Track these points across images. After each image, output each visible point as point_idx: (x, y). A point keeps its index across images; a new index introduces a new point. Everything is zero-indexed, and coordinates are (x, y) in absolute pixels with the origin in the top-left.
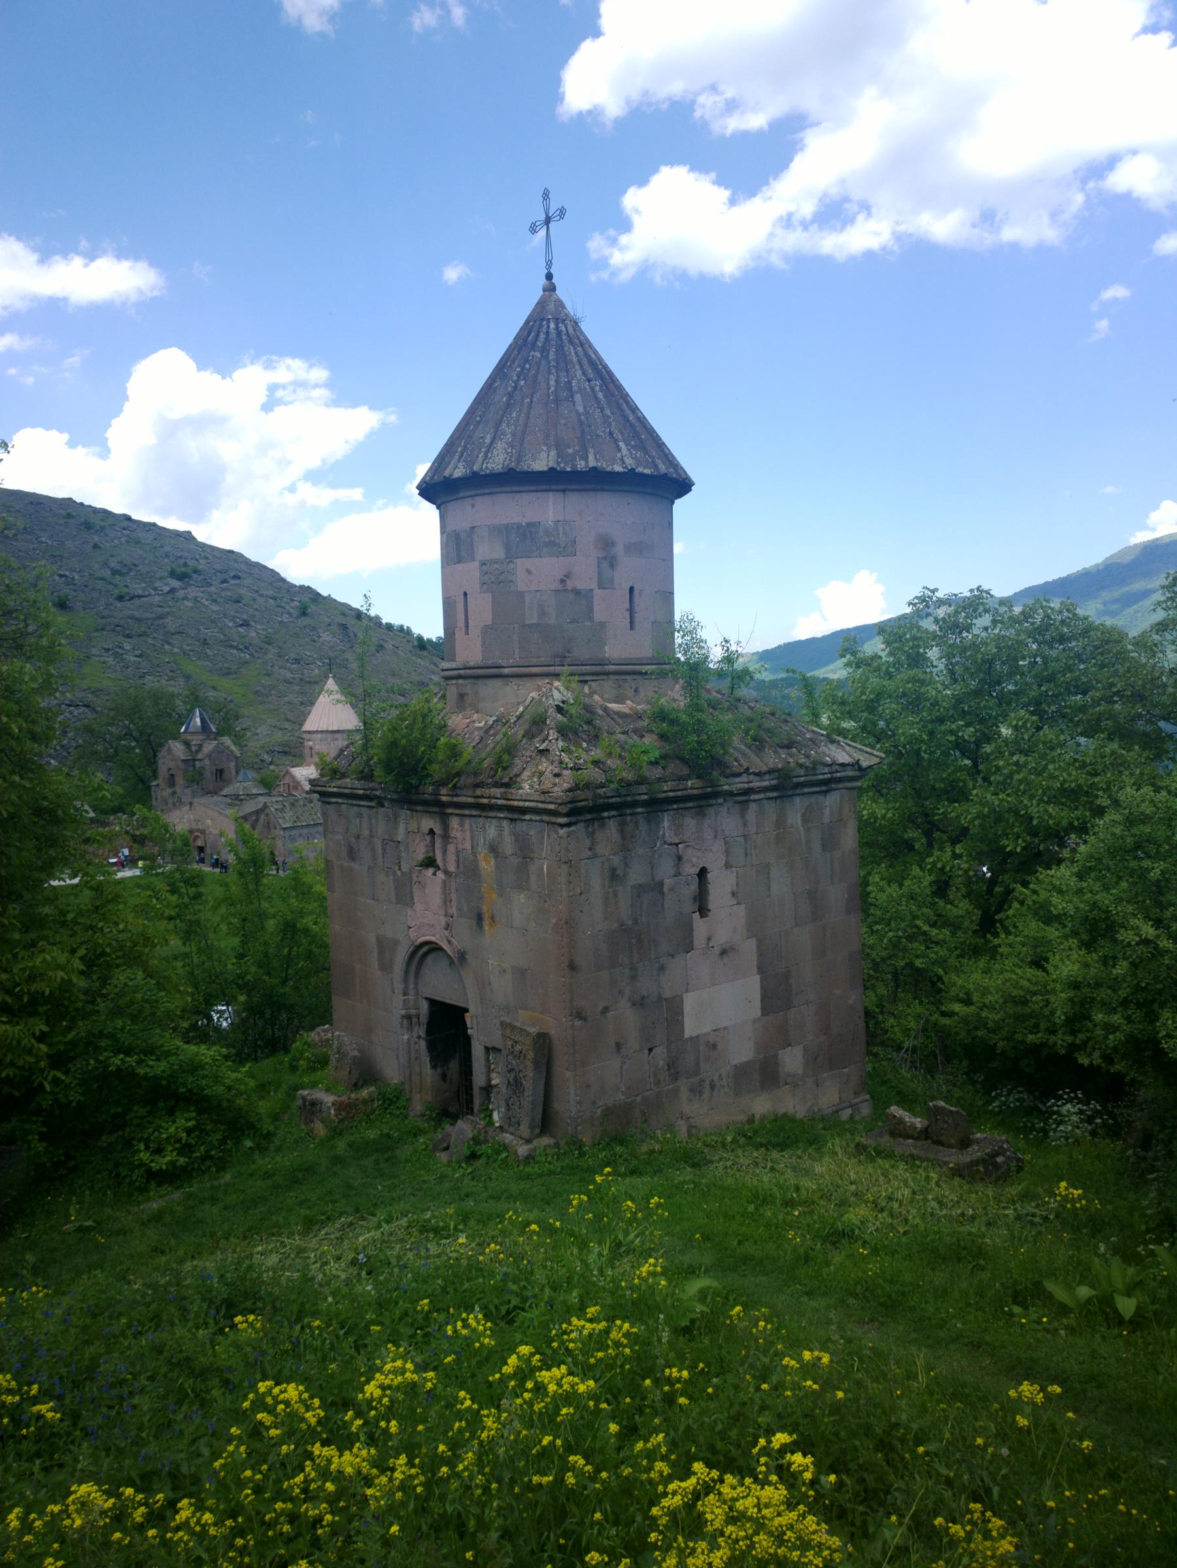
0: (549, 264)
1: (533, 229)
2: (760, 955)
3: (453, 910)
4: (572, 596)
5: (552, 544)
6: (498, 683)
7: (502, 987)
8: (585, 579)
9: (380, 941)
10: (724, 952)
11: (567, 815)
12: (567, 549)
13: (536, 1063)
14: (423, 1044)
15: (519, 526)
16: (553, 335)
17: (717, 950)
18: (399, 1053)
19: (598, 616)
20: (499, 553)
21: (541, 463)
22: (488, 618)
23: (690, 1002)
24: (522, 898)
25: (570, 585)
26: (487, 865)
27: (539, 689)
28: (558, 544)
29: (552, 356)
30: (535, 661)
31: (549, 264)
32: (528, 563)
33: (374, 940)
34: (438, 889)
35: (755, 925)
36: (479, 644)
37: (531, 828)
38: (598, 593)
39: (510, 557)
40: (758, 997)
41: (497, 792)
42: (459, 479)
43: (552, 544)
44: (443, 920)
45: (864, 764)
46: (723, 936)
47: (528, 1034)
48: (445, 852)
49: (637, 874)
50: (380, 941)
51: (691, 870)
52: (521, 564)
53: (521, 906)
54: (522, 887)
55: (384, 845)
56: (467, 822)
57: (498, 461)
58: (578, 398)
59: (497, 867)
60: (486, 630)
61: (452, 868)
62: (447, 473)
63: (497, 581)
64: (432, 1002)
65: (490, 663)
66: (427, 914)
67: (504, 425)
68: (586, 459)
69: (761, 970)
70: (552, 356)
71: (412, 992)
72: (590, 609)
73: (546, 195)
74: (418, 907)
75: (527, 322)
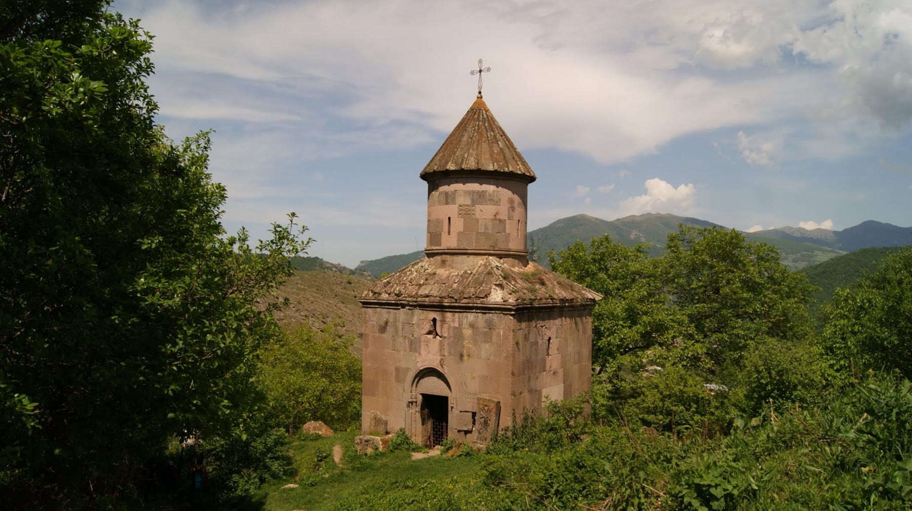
0: (480, 88)
1: (472, 73)
3: (446, 354)
5: (491, 200)
6: (465, 257)
7: (473, 386)
8: (503, 216)
9: (397, 370)
10: (554, 373)
12: (497, 203)
14: (418, 415)
15: (478, 192)
19: (508, 231)
20: (469, 202)
23: (545, 392)
24: (487, 346)
25: (498, 217)
26: (467, 332)
31: (480, 88)
32: (481, 207)
35: (563, 364)
36: (456, 239)
37: (494, 317)
38: (508, 221)
40: (562, 393)
43: (491, 200)
44: (439, 358)
46: (553, 368)
48: (442, 327)
49: (532, 338)
50: (397, 370)
51: (546, 338)
52: (478, 208)
53: (486, 349)
59: (473, 333)
60: (459, 234)
61: (446, 335)
63: (466, 213)
64: (422, 394)
66: (429, 356)
69: (564, 383)
73: (480, 61)
74: (423, 352)
75: (472, 109)
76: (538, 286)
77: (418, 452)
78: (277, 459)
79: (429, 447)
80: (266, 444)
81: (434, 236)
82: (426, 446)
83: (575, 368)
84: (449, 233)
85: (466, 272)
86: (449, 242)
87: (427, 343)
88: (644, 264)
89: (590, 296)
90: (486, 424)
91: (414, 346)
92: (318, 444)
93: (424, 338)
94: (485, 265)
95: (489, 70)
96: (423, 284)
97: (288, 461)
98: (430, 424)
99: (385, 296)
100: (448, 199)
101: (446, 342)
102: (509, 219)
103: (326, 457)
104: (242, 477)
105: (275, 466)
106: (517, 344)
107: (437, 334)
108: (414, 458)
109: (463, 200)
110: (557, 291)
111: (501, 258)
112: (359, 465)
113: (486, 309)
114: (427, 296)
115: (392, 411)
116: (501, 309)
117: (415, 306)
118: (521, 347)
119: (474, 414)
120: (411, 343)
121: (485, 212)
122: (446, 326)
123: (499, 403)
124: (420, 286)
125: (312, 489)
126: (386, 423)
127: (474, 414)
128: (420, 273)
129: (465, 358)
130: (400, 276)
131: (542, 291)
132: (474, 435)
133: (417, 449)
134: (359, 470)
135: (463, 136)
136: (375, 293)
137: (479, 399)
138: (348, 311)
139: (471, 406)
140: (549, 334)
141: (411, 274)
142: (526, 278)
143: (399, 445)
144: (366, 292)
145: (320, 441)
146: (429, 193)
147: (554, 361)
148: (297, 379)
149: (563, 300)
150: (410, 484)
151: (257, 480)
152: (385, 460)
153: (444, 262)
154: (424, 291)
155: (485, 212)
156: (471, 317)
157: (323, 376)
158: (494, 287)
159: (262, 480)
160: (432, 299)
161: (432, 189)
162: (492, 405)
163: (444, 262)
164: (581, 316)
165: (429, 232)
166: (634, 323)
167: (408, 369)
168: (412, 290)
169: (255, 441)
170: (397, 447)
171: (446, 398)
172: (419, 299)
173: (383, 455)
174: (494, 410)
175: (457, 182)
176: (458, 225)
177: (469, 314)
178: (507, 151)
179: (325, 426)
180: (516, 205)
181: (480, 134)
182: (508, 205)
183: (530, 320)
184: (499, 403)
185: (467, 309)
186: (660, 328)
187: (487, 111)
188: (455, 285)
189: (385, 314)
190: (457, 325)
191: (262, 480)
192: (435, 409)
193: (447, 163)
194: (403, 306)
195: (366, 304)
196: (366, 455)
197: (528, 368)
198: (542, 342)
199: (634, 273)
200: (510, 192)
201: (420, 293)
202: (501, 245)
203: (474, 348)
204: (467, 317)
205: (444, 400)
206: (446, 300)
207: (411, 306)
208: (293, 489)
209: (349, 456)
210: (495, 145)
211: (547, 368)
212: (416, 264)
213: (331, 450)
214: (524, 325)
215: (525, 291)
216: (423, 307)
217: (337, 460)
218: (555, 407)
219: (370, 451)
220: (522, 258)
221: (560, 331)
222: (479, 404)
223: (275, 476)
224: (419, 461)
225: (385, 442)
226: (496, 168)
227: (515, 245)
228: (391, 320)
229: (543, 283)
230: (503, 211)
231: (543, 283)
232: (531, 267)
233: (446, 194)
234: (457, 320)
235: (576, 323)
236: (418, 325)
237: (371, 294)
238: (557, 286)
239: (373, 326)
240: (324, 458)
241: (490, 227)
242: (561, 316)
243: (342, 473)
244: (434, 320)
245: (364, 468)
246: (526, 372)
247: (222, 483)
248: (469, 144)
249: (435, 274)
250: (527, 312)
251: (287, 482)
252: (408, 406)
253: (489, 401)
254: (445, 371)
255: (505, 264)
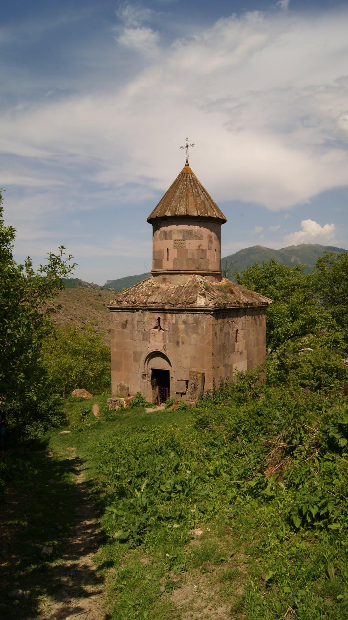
0: (187, 158)
1: (182, 148)
2: (247, 355)
3: (167, 341)
4: (201, 251)
5: (196, 236)
6: (179, 275)
7: (186, 363)
8: (205, 247)
9: (135, 353)
10: (241, 353)
11: (213, 311)
13: (202, 381)
14: (149, 383)
15: (187, 231)
16: (191, 178)
17: (239, 353)
18: (140, 386)
19: (208, 258)
20: (181, 238)
21: (195, 214)
22: (176, 256)
23: (234, 366)
24: (195, 336)
25: (201, 248)
26: (182, 327)
27: (191, 277)
28: (198, 237)
29: (192, 184)
30: (191, 269)
31: (187, 158)
32: (189, 241)
33: (132, 352)
34: (161, 335)
35: (247, 347)
36: (172, 263)
37: (199, 316)
38: (208, 251)
39: (184, 239)
40: (246, 366)
41: (189, 306)
42: (170, 217)
43: (196, 236)
44: (163, 344)
45: (269, 303)
46: (240, 349)
47: (200, 373)
49: (225, 330)
50: (135, 353)
51: (235, 330)
52: (187, 241)
53: (194, 338)
54: (195, 333)
55: (138, 322)
56: (174, 315)
57: (182, 212)
58: (201, 196)
60: (175, 260)
61: (167, 329)
62: (166, 214)
63: (179, 245)
65: (176, 269)
66: (156, 343)
67: (182, 202)
68: (207, 213)
70: (192, 184)
71: (146, 367)
72: (206, 255)
73: (187, 139)
75: (182, 173)
76: (229, 295)
77: (150, 407)
78: (56, 414)
79: (157, 404)
80: (48, 405)
81: (157, 262)
82: (155, 404)
83: (255, 349)
84: (168, 260)
85: (180, 286)
86: (168, 265)
87: (155, 333)
88: (301, 278)
89: (264, 301)
90: (195, 388)
91: (146, 337)
92: (83, 404)
93: (152, 331)
94: (193, 281)
95: (193, 145)
96: (151, 295)
97: (63, 415)
98: (157, 389)
99: (125, 303)
100: (167, 236)
101: (167, 334)
102: (209, 249)
103: (88, 412)
104: (33, 427)
105: (55, 419)
106: (215, 334)
107: (161, 329)
108: (147, 412)
109: (177, 236)
110: (242, 298)
111: (203, 276)
112: (110, 417)
113: (194, 311)
114: (154, 303)
115: (131, 381)
116: (204, 311)
117: (145, 310)
118: (218, 336)
119: (187, 382)
120: (144, 335)
121: (192, 245)
122: (167, 323)
123: (204, 374)
124: (149, 296)
125: (80, 433)
126: (128, 389)
127: (187, 382)
128: (148, 287)
129: (181, 344)
130: (135, 290)
131: (231, 298)
132: (188, 395)
133: (149, 406)
134: (110, 420)
135: (176, 192)
136: (118, 301)
137: (190, 372)
138: (99, 314)
139: (184, 376)
140: (237, 327)
141: (142, 288)
142: (221, 289)
143: (137, 403)
144: (112, 301)
145: (84, 402)
146: (154, 232)
147: (240, 345)
148: (67, 360)
149: (246, 304)
150: (145, 429)
151: (42, 429)
152: (128, 414)
153: (164, 279)
154: (152, 299)
155: (192, 245)
156: (184, 316)
157: (84, 358)
158: (199, 295)
159: (46, 429)
160: (157, 304)
161: (155, 229)
162: (199, 375)
163: (164, 279)
164: (258, 314)
165: (154, 259)
166: (295, 318)
167: (142, 353)
168: (143, 299)
169: (40, 403)
170: (136, 404)
171: (168, 371)
172: (148, 305)
173: (126, 410)
174: (201, 379)
175: (172, 224)
176: (174, 254)
177: (182, 315)
178: (206, 202)
179: (87, 392)
180: (213, 239)
181: (188, 190)
182: (207, 240)
183: (224, 317)
184: (204, 374)
185: (181, 311)
186: (313, 322)
187: (192, 174)
188: (173, 295)
189: (125, 315)
190: (174, 322)
191: (46, 429)
192: (161, 379)
193: (165, 211)
194: (138, 310)
195: (112, 309)
196: (115, 410)
197: (223, 350)
198: (232, 333)
199: (293, 285)
200: (209, 231)
201: (149, 300)
202: (204, 267)
203: (186, 337)
204: (181, 316)
205: (167, 372)
206: (167, 306)
207: (143, 310)
208: (67, 434)
209: (104, 412)
210: (198, 198)
211: (236, 350)
212: (146, 281)
213: (91, 408)
214: (220, 321)
215: (220, 298)
216: (151, 310)
217: (95, 414)
218: (242, 375)
219: (117, 407)
220: (218, 276)
221: (244, 325)
222: (190, 375)
223: (54, 426)
224: (151, 413)
225: (127, 402)
226: (199, 214)
227: (213, 267)
228: (130, 320)
229: (232, 293)
230: (204, 243)
231: (232, 293)
232: (224, 282)
233: (165, 233)
234: (174, 318)
235: (255, 319)
236: (148, 323)
237: (115, 302)
238: (242, 295)
239: (117, 324)
240: (87, 413)
241: (196, 255)
242: (245, 315)
243: (99, 423)
244: (159, 319)
245: (114, 419)
246: (222, 353)
247: (19, 431)
248: (180, 198)
249: (158, 288)
250: (221, 312)
251: (63, 429)
252: (143, 377)
253: (197, 372)
254: (167, 353)
255: (207, 280)
